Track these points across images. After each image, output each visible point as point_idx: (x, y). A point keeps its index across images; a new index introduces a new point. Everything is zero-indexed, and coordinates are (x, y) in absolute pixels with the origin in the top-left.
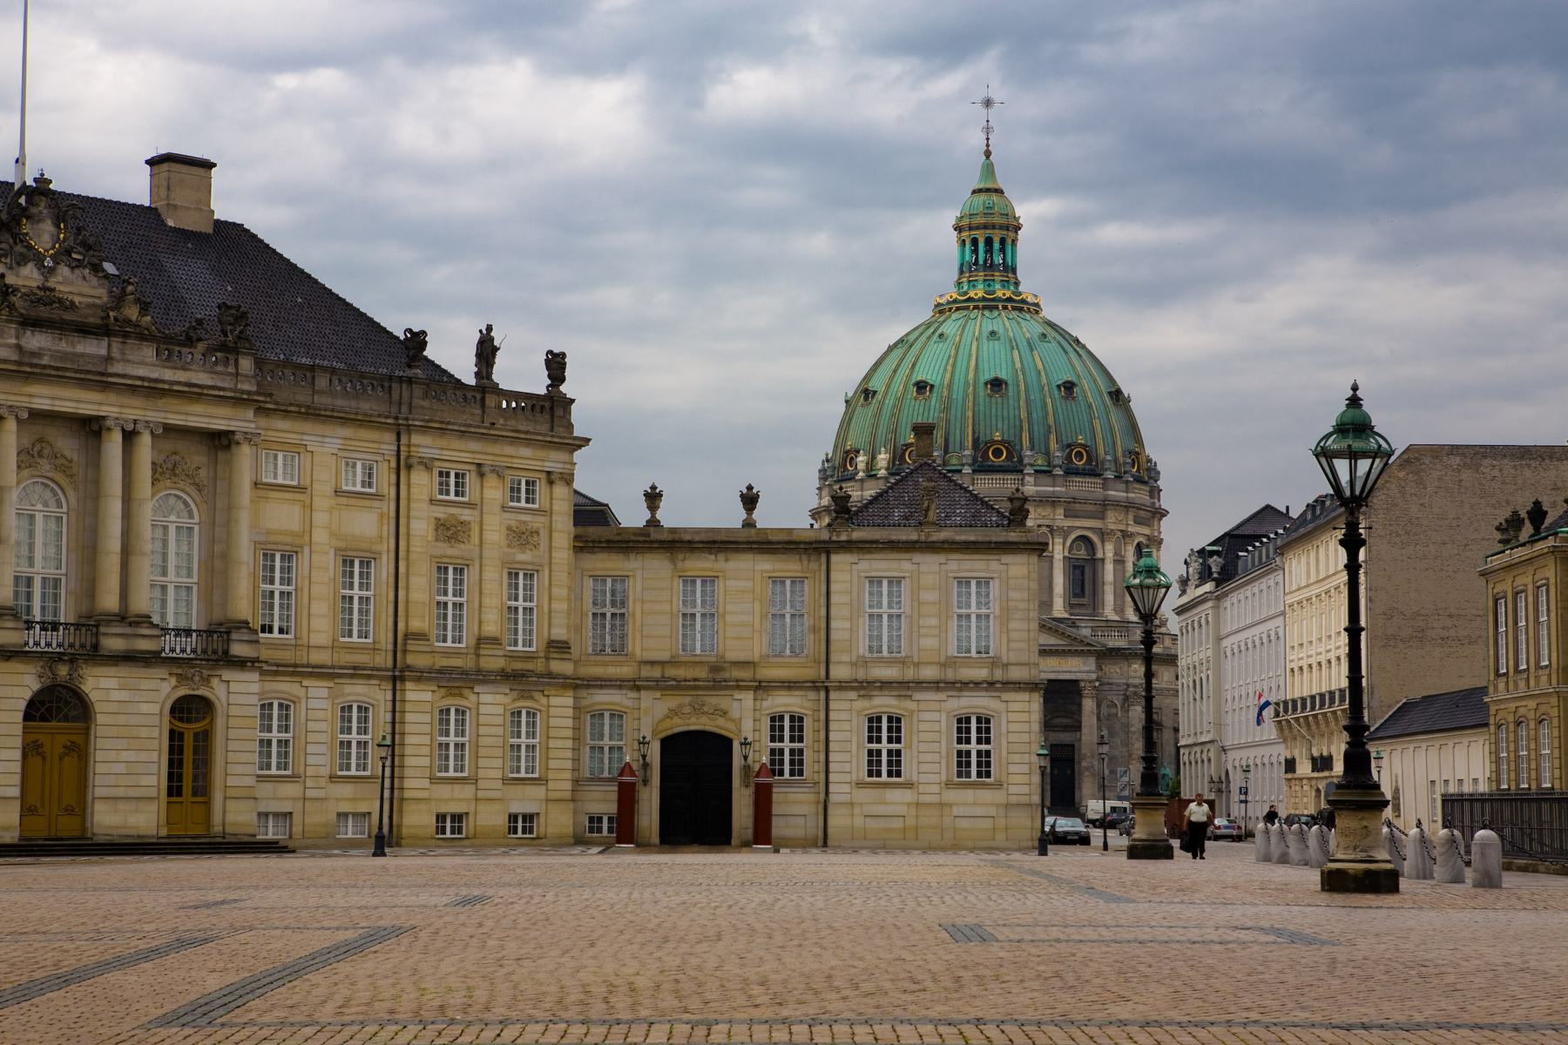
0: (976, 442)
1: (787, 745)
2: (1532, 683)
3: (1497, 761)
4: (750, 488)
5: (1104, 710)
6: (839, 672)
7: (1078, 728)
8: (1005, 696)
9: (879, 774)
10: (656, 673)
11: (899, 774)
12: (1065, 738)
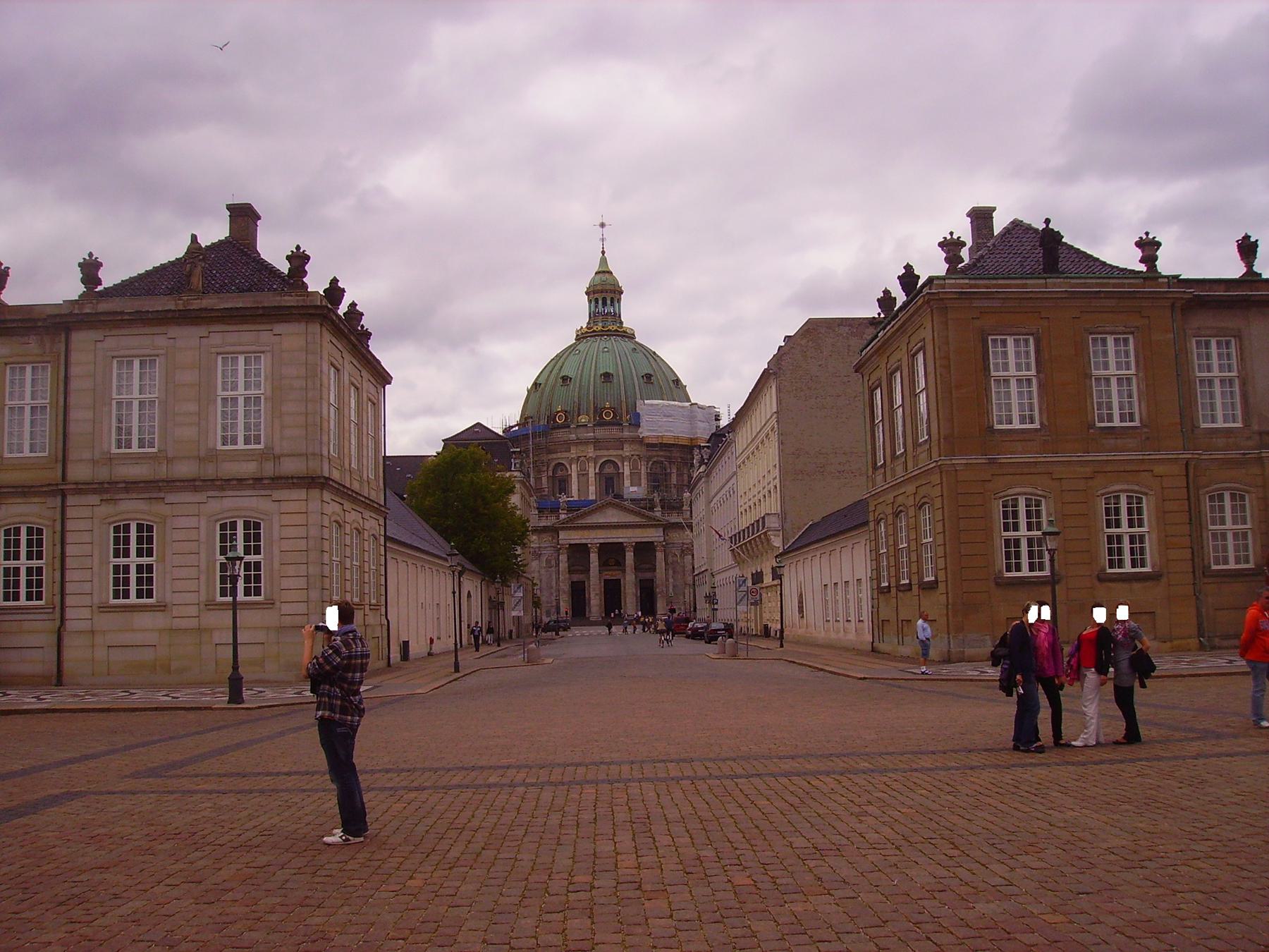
0: (595, 408)
1: (23, 563)
2: (910, 464)
3: (877, 558)
5: (670, 559)
6: (79, 472)
7: (655, 570)
8: (277, 494)
9: (127, 596)
11: (150, 595)
12: (648, 575)
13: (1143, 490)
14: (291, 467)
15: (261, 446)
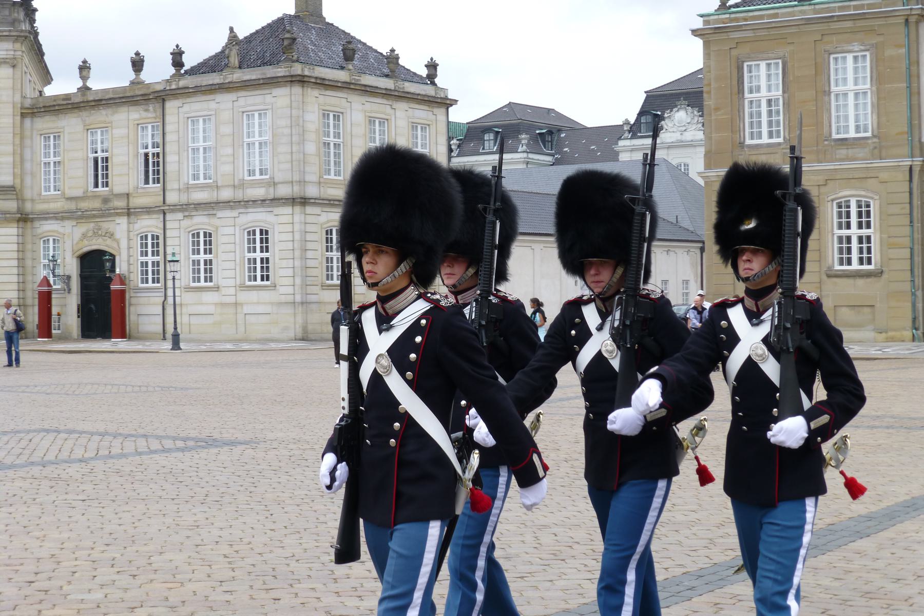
4: (137, 54)
10: (72, 206)
11: (211, 281)
13: (870, 195)
14: (284, 191)
15: (267, 177)
